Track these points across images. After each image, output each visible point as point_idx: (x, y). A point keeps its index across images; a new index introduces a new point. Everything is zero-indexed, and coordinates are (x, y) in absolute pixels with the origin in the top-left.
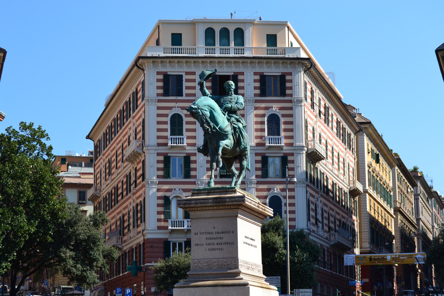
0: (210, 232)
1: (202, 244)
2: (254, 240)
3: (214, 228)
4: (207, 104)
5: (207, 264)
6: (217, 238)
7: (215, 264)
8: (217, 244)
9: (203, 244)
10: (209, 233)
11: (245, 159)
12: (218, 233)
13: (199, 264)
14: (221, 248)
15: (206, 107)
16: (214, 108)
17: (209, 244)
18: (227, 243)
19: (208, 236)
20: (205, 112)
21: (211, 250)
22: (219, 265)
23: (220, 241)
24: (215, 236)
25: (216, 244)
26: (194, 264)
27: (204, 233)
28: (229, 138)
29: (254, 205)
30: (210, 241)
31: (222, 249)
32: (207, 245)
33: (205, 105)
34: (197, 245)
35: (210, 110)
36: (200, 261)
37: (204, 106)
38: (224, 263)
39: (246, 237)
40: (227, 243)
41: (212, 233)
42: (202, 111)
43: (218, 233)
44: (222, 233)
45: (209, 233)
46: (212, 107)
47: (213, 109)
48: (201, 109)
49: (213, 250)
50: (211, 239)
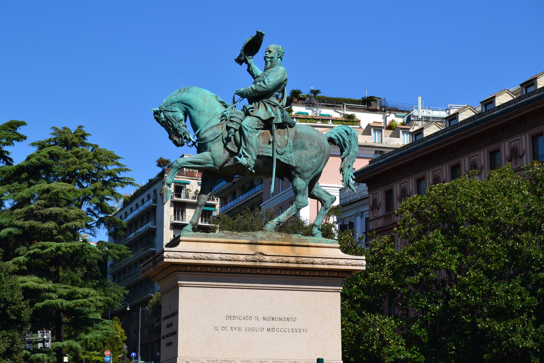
2: (295, 319)
4: (178, 100)
11: (297, 176)
15: (175, 105)
16: (190, 104)
20: (170, 114)
28: (208, 149)
29: (226, 260)
33: (172, 103)
35: (185, 108)
37: (172, 104)
39: (229, 317)
42: (166, 114)
46: (186, 102)
47: (189, 106)
48: (164, 110)
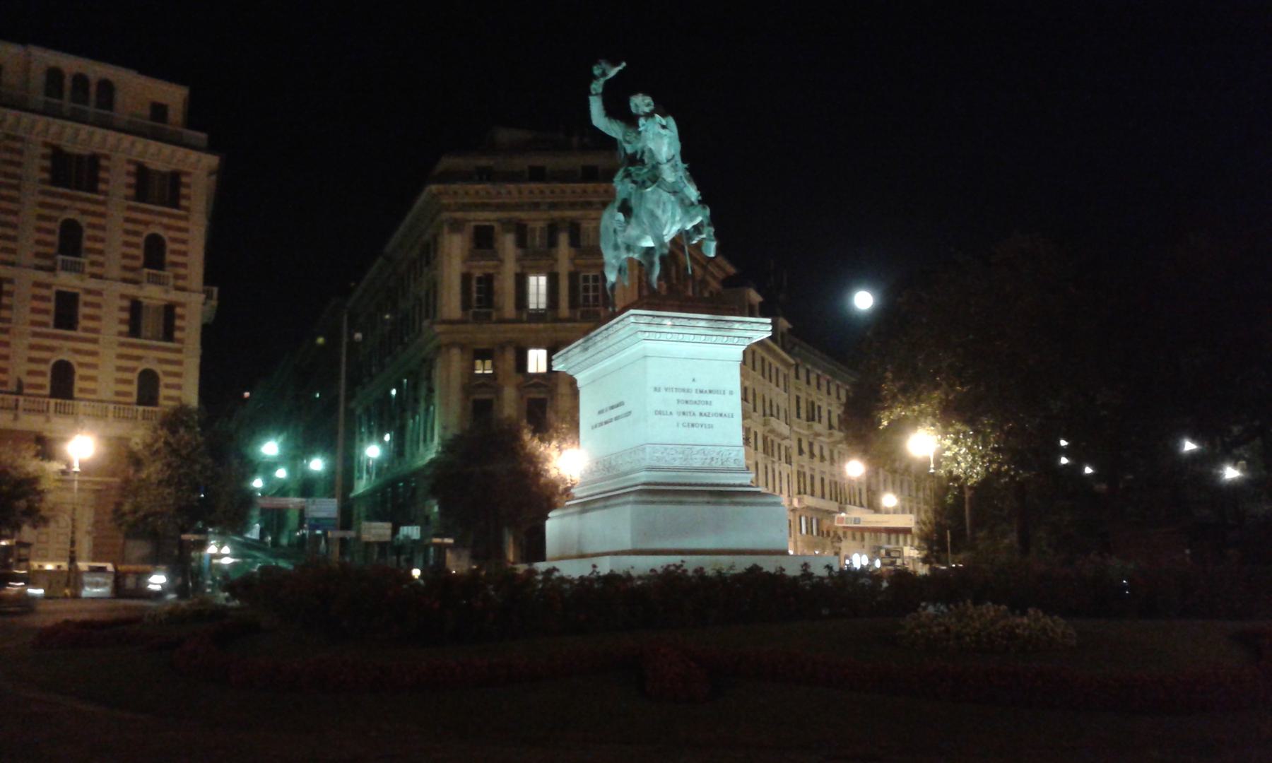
0: (686, 387)
1: (669, 413)
3: (694, 380)
5: (681, 456)
6: (699, 401)
7: (698, 456)
8: (701, 414)
9: (671, 413)
10: (683, 390)
12: (701, 392)
13: (665, 454)
14: (707, 423)
17: (684, 413)
18: (721, 415)
19: (682, 396)
21: (688, 425)
22: (706, 459)
23: (705, 409)
24: (696, 397)
25: (697, 414)
26: (654, 452)
27: (674, 390)
30: (686, 408)
31: (711, 426)
32: (679, 415)
34: (659, 413)
36: (666, 449)
38: (718, 456)
40: (721, 415)
41: (688, 391)
43: (701, 392)
44: (710, 392)
45: (683, 390)
49: (693, 425)
50: (687, 402)
